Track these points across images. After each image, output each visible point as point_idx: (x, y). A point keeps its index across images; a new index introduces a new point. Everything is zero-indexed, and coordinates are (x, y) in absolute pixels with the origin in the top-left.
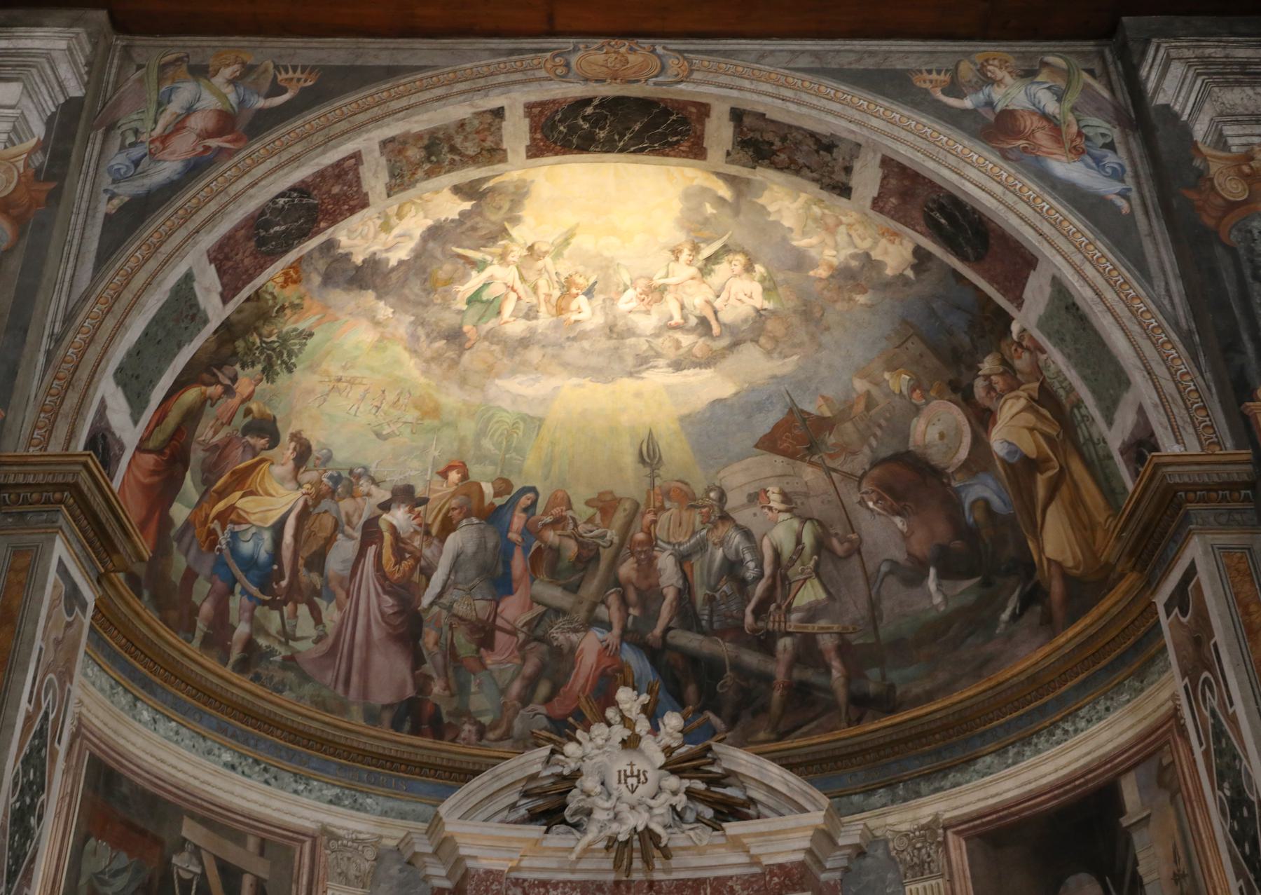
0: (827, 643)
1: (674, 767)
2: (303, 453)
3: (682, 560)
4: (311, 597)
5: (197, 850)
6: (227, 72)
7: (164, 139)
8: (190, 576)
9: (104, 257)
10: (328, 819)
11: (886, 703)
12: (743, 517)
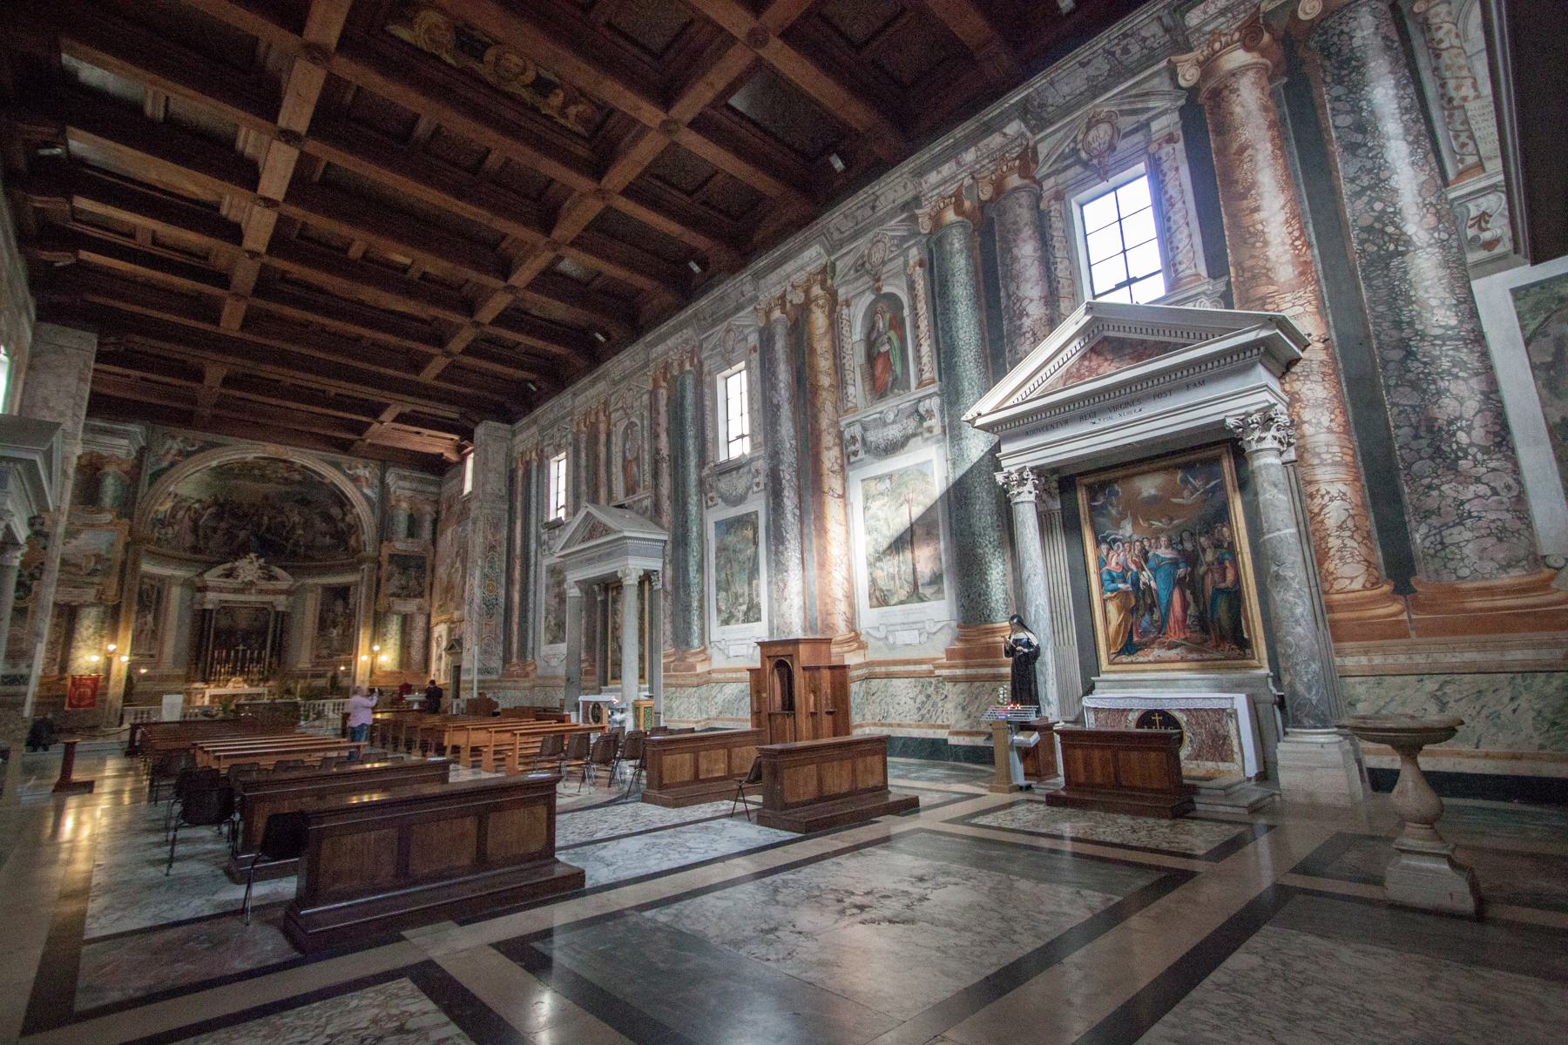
1: (261, 568)
3: (270, 519)
4: (171, 524)
9: (150, 484)
11: (312, 559)
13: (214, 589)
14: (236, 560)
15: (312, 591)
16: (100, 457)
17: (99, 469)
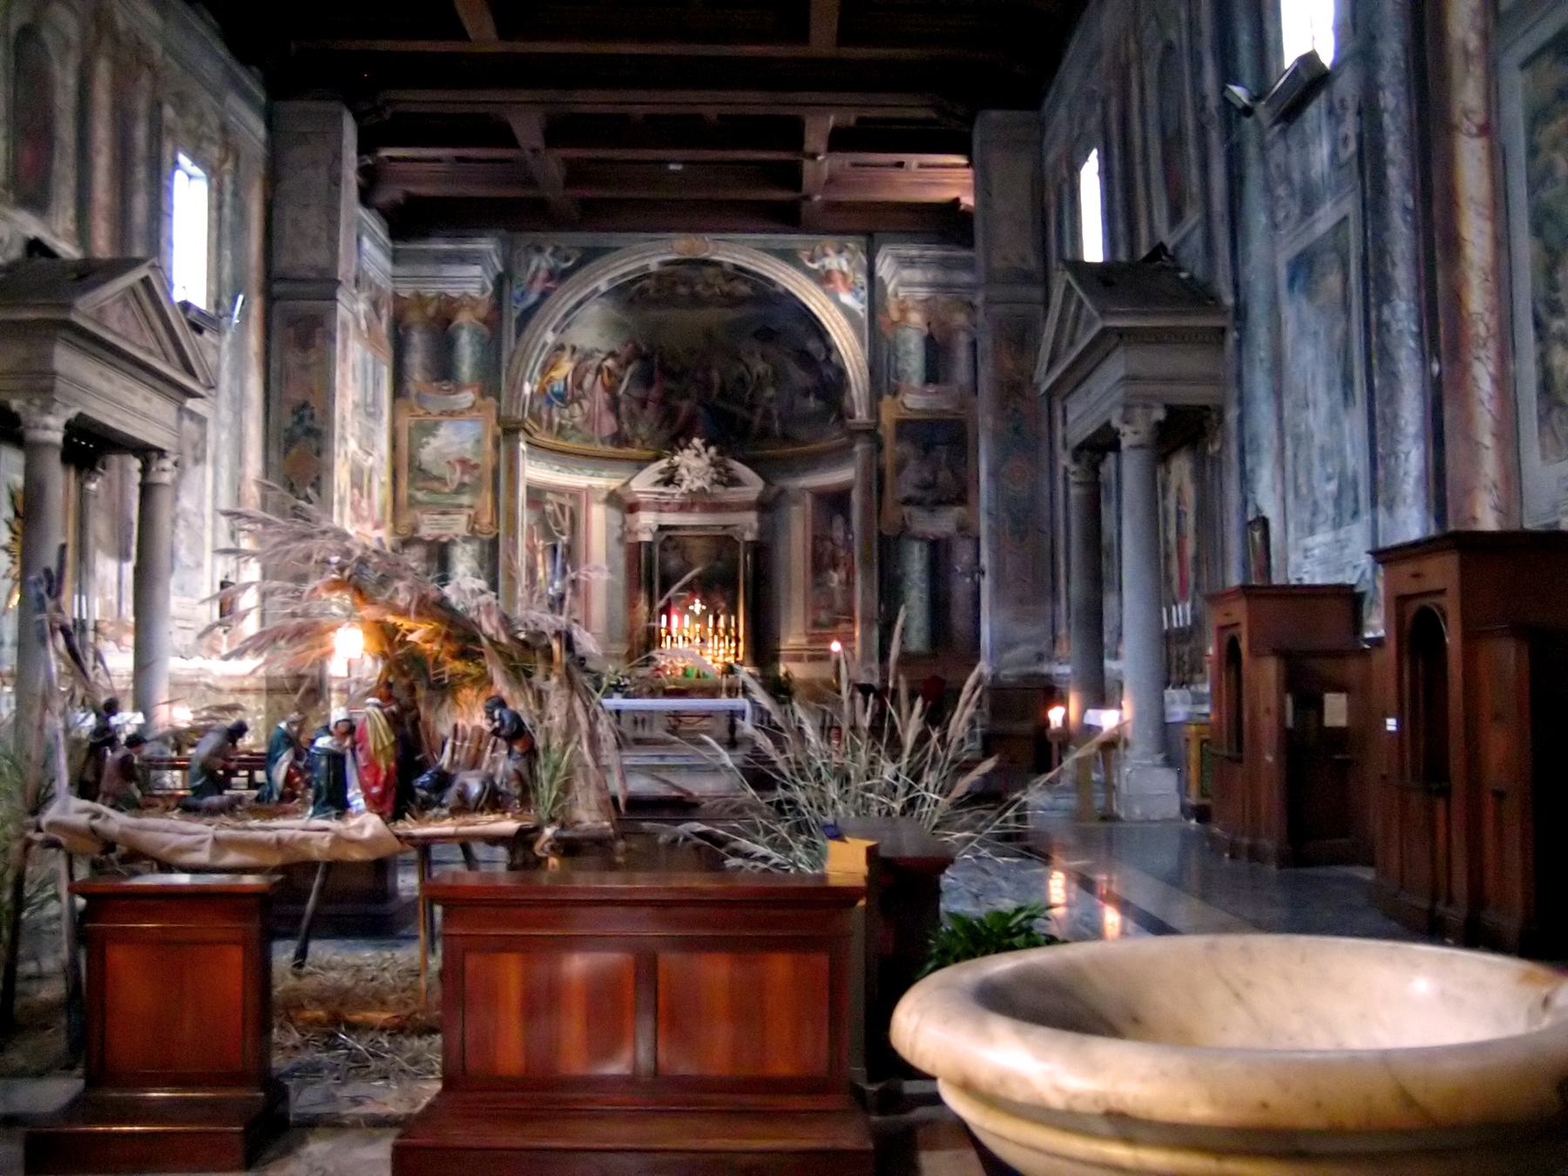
0: (775, 412)
2: (574, 349)
4: (576, 400)
5: (551, 503)
6: (549, 250)
7: (531, 282)
8: (540, 408)
9: (519, 333)
10: (590, 482)
12: (747, 360)
13: (647, 507)
14: (675, 453)
15: (796, 502)
16: (450, 301)
17: (449, 322)
